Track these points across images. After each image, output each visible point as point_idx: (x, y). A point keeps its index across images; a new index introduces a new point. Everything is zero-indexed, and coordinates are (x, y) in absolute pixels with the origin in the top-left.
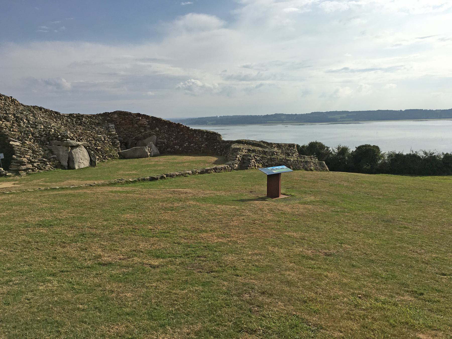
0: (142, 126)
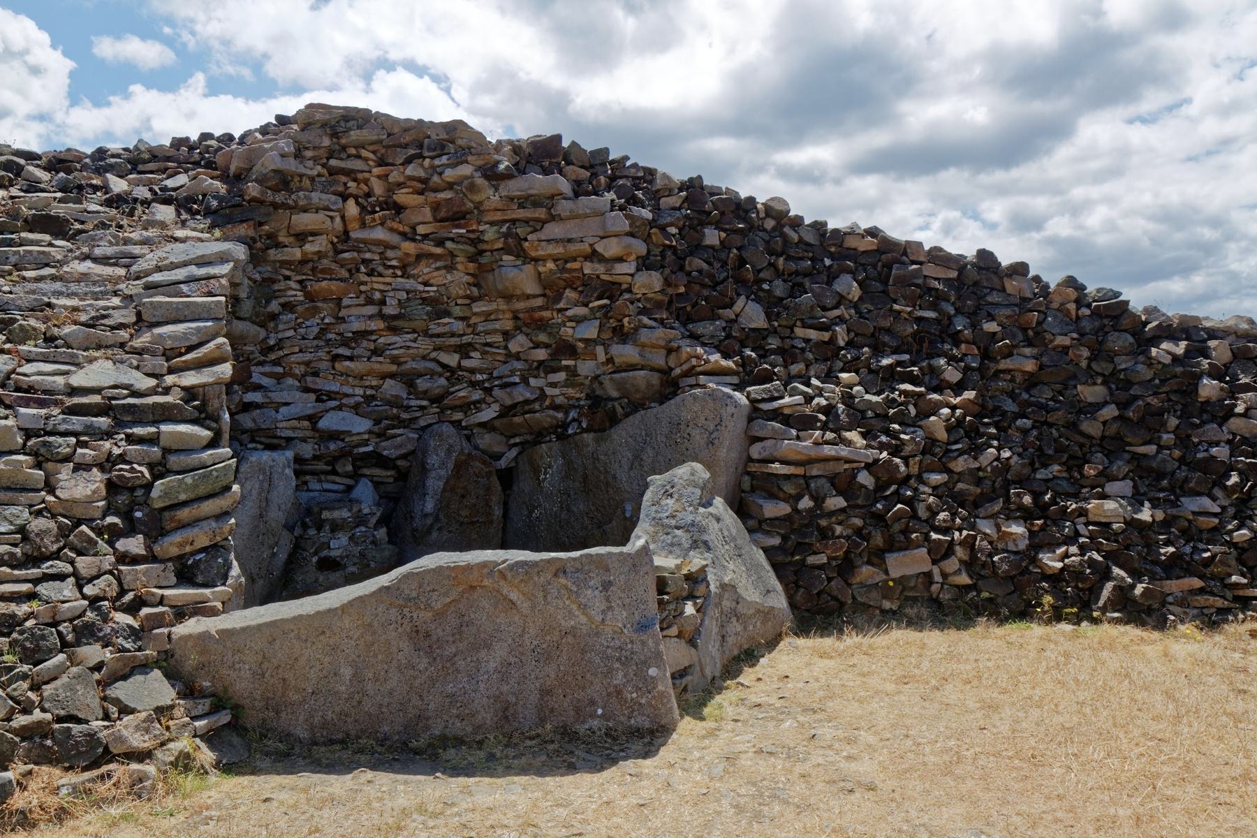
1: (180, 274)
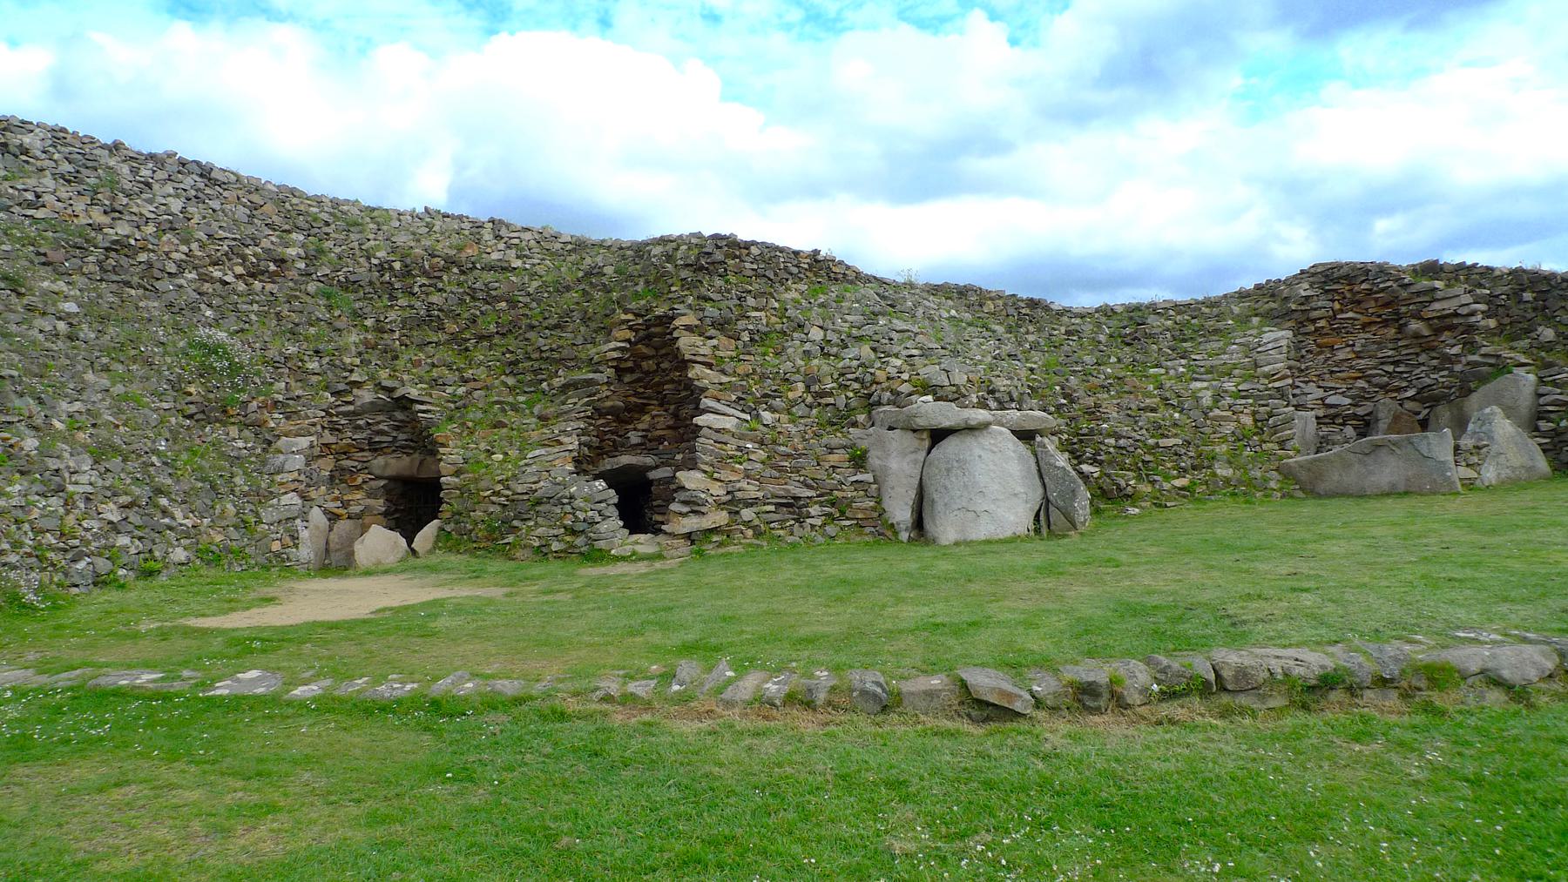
0: (1451, 328)
1: (1270, 346)
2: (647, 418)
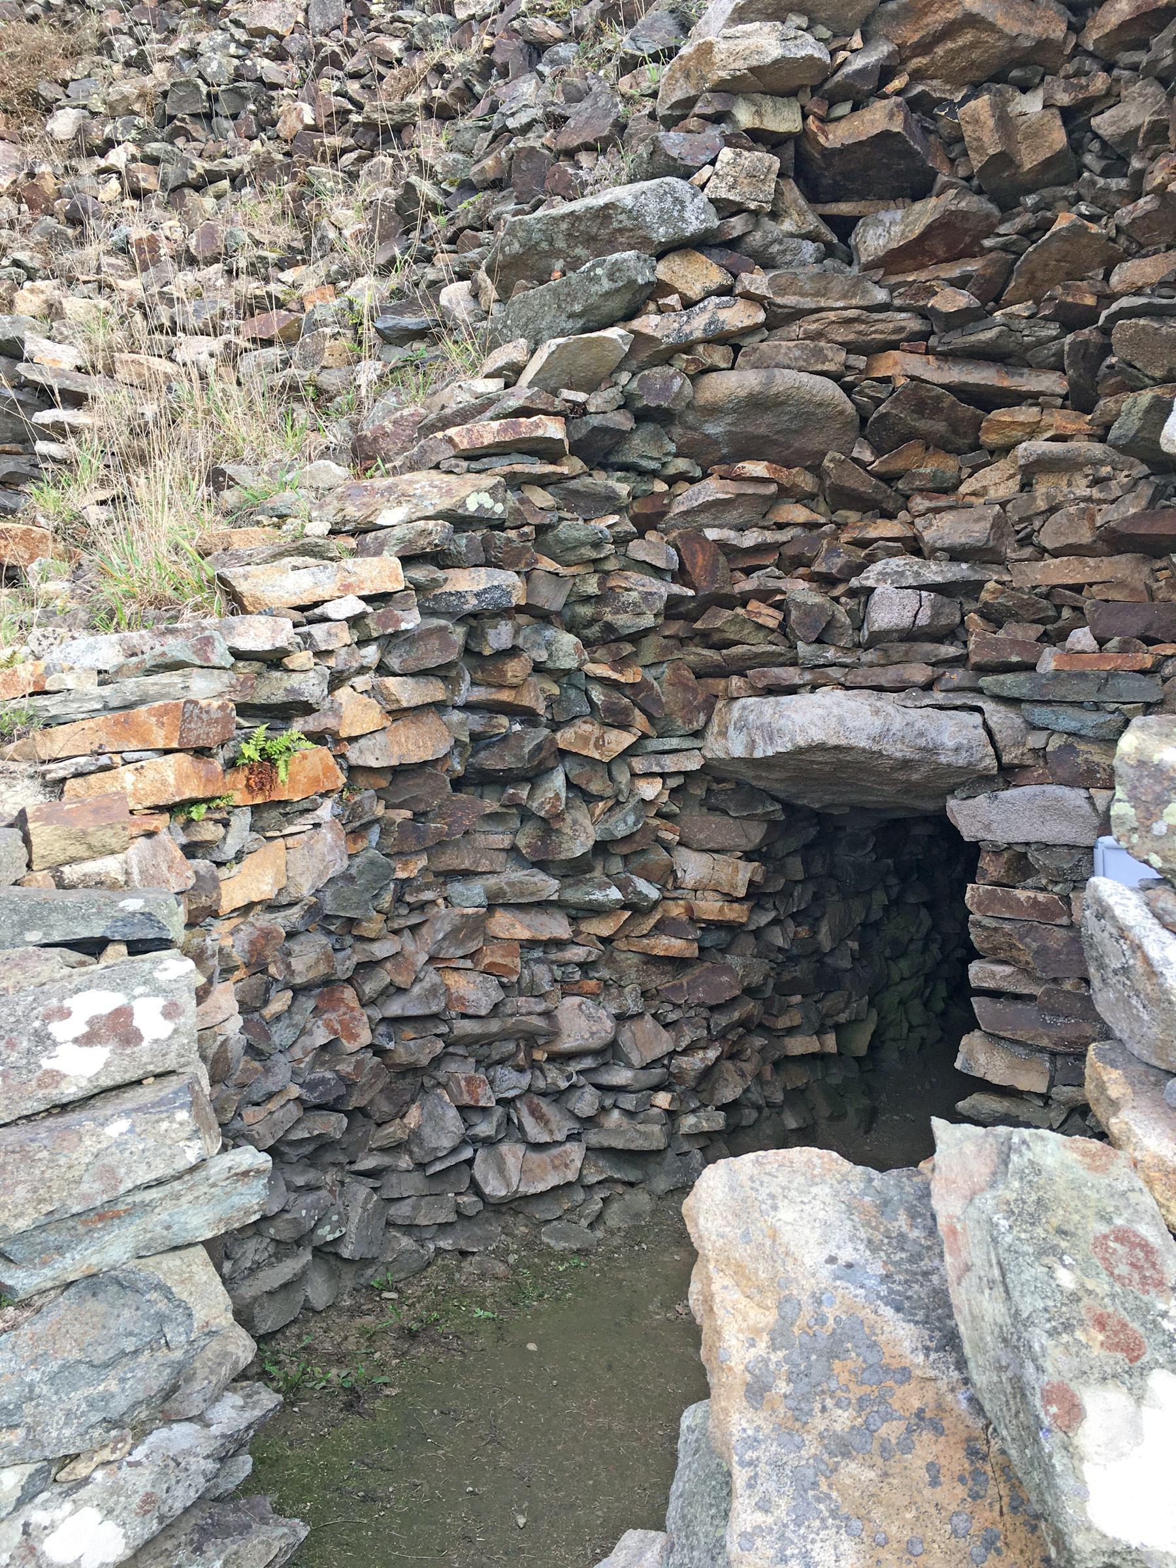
2: (997, 480)
